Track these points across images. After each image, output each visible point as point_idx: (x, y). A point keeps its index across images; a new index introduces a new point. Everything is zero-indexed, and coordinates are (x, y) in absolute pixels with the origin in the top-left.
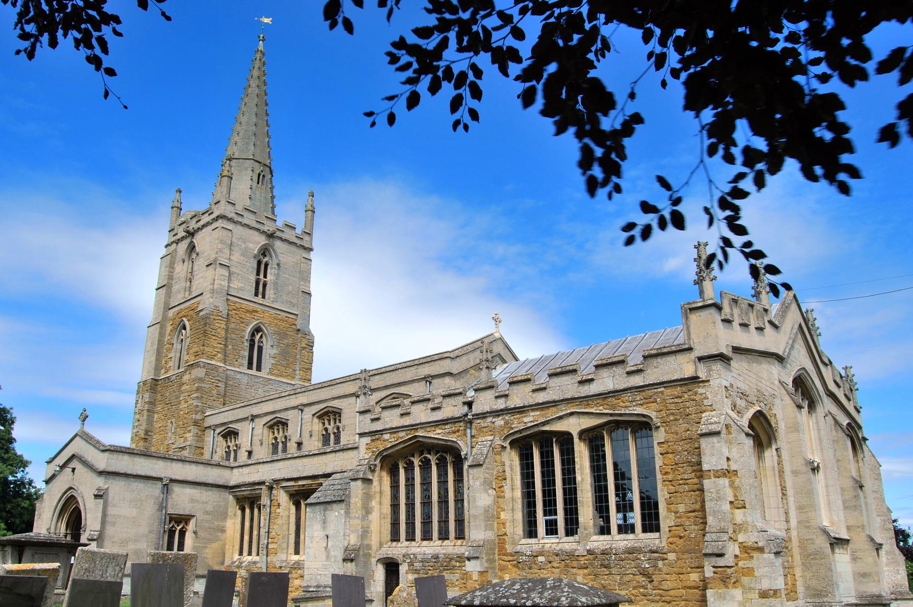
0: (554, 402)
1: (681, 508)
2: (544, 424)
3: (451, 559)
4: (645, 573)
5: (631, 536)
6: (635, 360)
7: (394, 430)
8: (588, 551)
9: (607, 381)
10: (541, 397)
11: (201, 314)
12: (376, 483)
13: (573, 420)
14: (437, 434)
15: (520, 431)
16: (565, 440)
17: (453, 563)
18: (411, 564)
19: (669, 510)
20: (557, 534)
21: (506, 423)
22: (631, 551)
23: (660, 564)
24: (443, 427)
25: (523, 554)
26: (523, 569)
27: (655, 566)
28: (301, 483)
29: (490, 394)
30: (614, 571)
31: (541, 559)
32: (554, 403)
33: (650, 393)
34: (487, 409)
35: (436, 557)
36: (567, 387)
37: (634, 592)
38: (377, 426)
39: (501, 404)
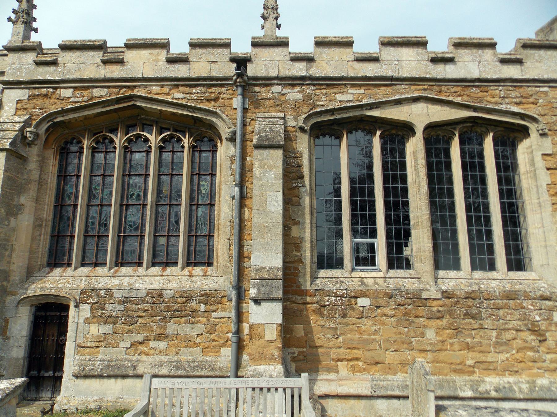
0: (392, 79)
2: (371, 106)
3: (189, 299)
4: (534, 330)
5: (493, 274)
6: (506, 47)
7: (83, 84)
8: (443, 292)
9: (469, 66)
10: (370, 70)
12: (33, 165)
13: (420, 107)
15: (332, 112)
16: (396, 134)
17: (193, 304)
18: (99, 306)
20: (374, 264)
21: (307, 98)
24: (187, 89)
25: (329, 293)
26: (331, 317)
27: (549, 319)
29: (277, 53)
30: (488, 323)
31: (363, 302)
32: (391, 81)
33: (531, 90)
34: (274, 73)
35: (159, 294)
36: (409, 63)
37: (519, 356)
38: (48, 73)
39: (300, 69)
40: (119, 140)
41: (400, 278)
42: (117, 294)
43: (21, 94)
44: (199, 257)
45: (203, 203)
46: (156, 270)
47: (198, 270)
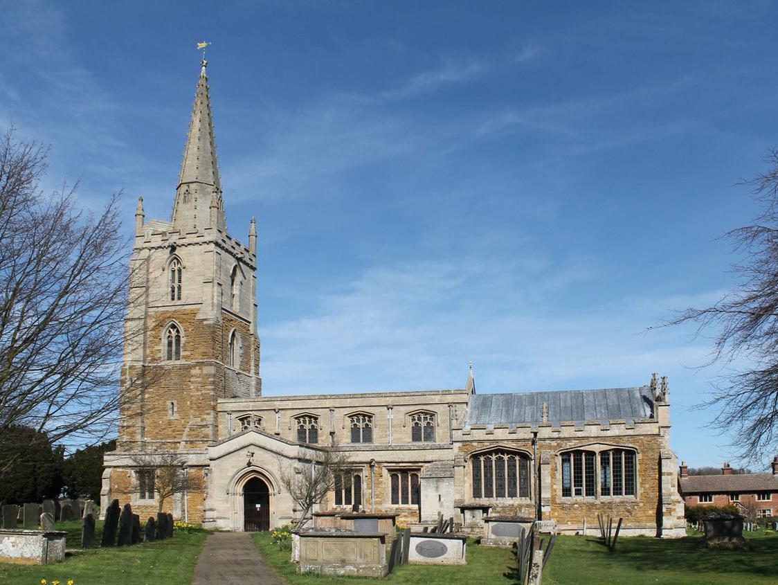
1: (647, 486)
4: (628, 511)
5: (620, 496)
11: (205, 323)
14: (513, 445)
19: (641, 487)
22: (622, 502)
23: (636, 507)
27: (634, 508)
28: (401, 465)
35: (513, 505)
40: (494, 457)
41: (590, 499)
42: (500, 505)
43: (460, 445)
44: (525, 493)
45: (525, 478)
46: (510, 498)
47: (523, 498)
